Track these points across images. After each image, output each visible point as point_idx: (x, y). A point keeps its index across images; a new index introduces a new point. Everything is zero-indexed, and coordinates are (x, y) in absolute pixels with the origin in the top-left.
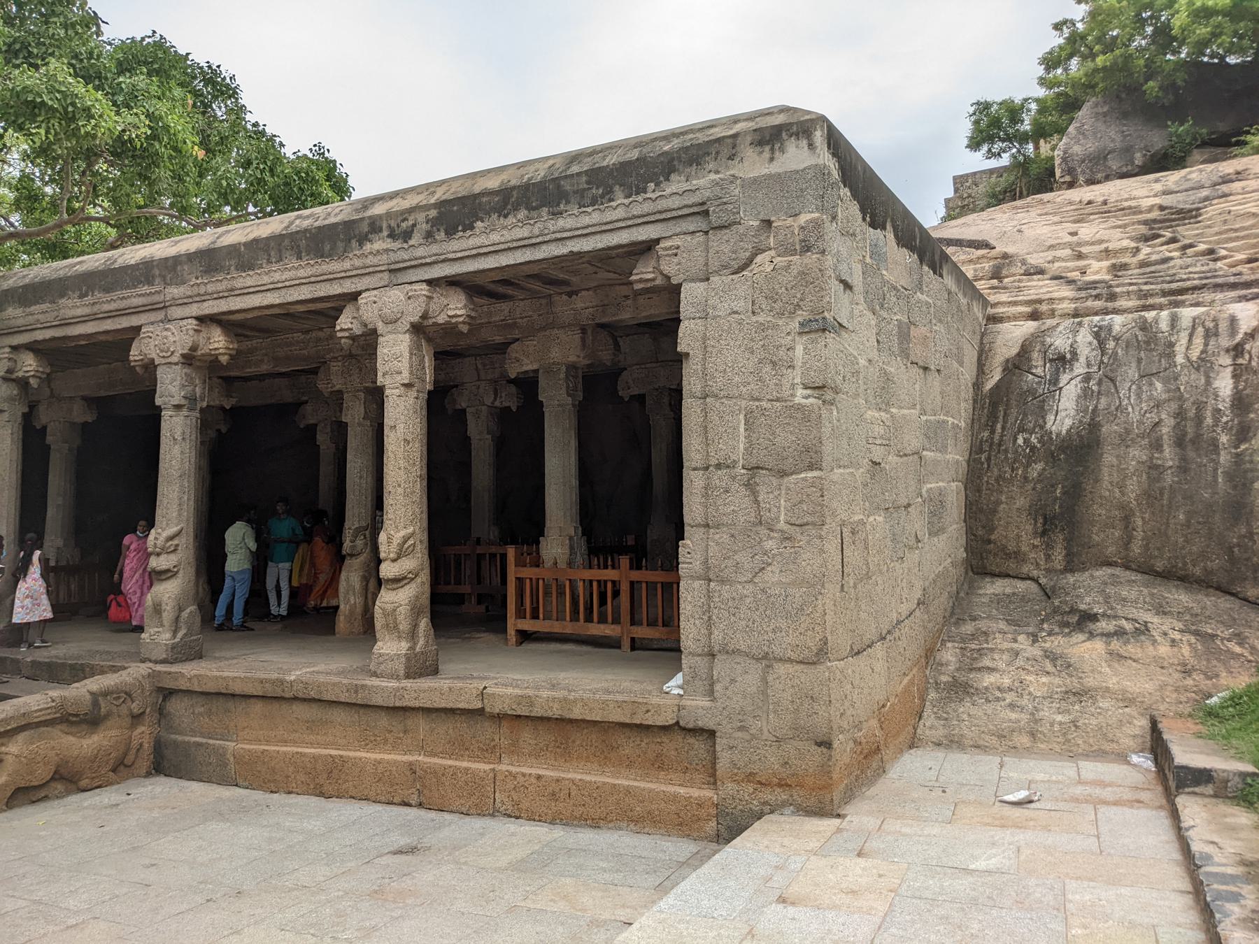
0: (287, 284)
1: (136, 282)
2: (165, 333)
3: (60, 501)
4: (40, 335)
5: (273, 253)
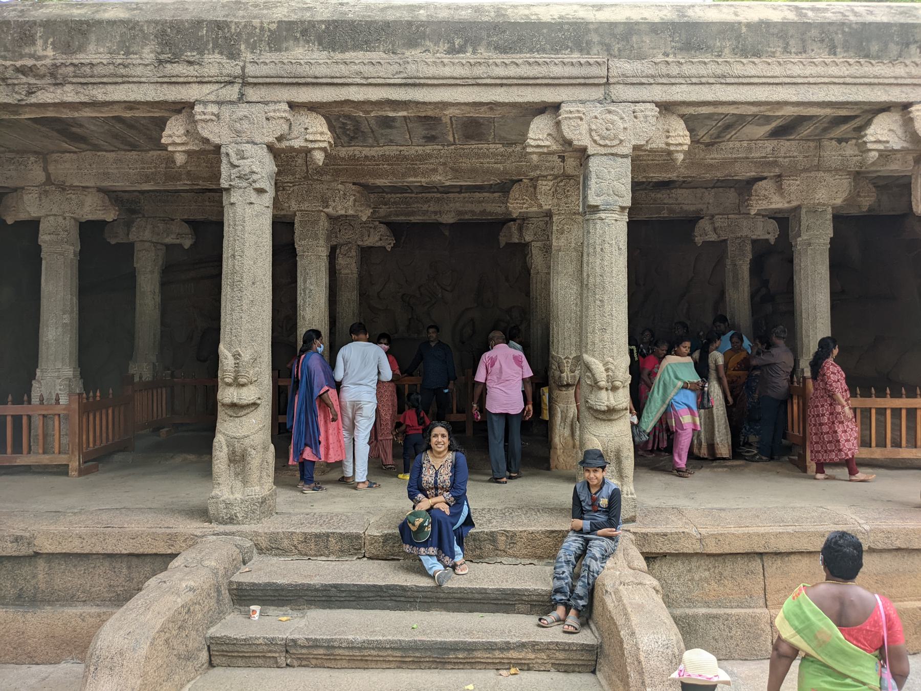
0: (812, 80)
1: (557, 46)
2: (609, 116)
3: (66, 319)
5: (792, 42)
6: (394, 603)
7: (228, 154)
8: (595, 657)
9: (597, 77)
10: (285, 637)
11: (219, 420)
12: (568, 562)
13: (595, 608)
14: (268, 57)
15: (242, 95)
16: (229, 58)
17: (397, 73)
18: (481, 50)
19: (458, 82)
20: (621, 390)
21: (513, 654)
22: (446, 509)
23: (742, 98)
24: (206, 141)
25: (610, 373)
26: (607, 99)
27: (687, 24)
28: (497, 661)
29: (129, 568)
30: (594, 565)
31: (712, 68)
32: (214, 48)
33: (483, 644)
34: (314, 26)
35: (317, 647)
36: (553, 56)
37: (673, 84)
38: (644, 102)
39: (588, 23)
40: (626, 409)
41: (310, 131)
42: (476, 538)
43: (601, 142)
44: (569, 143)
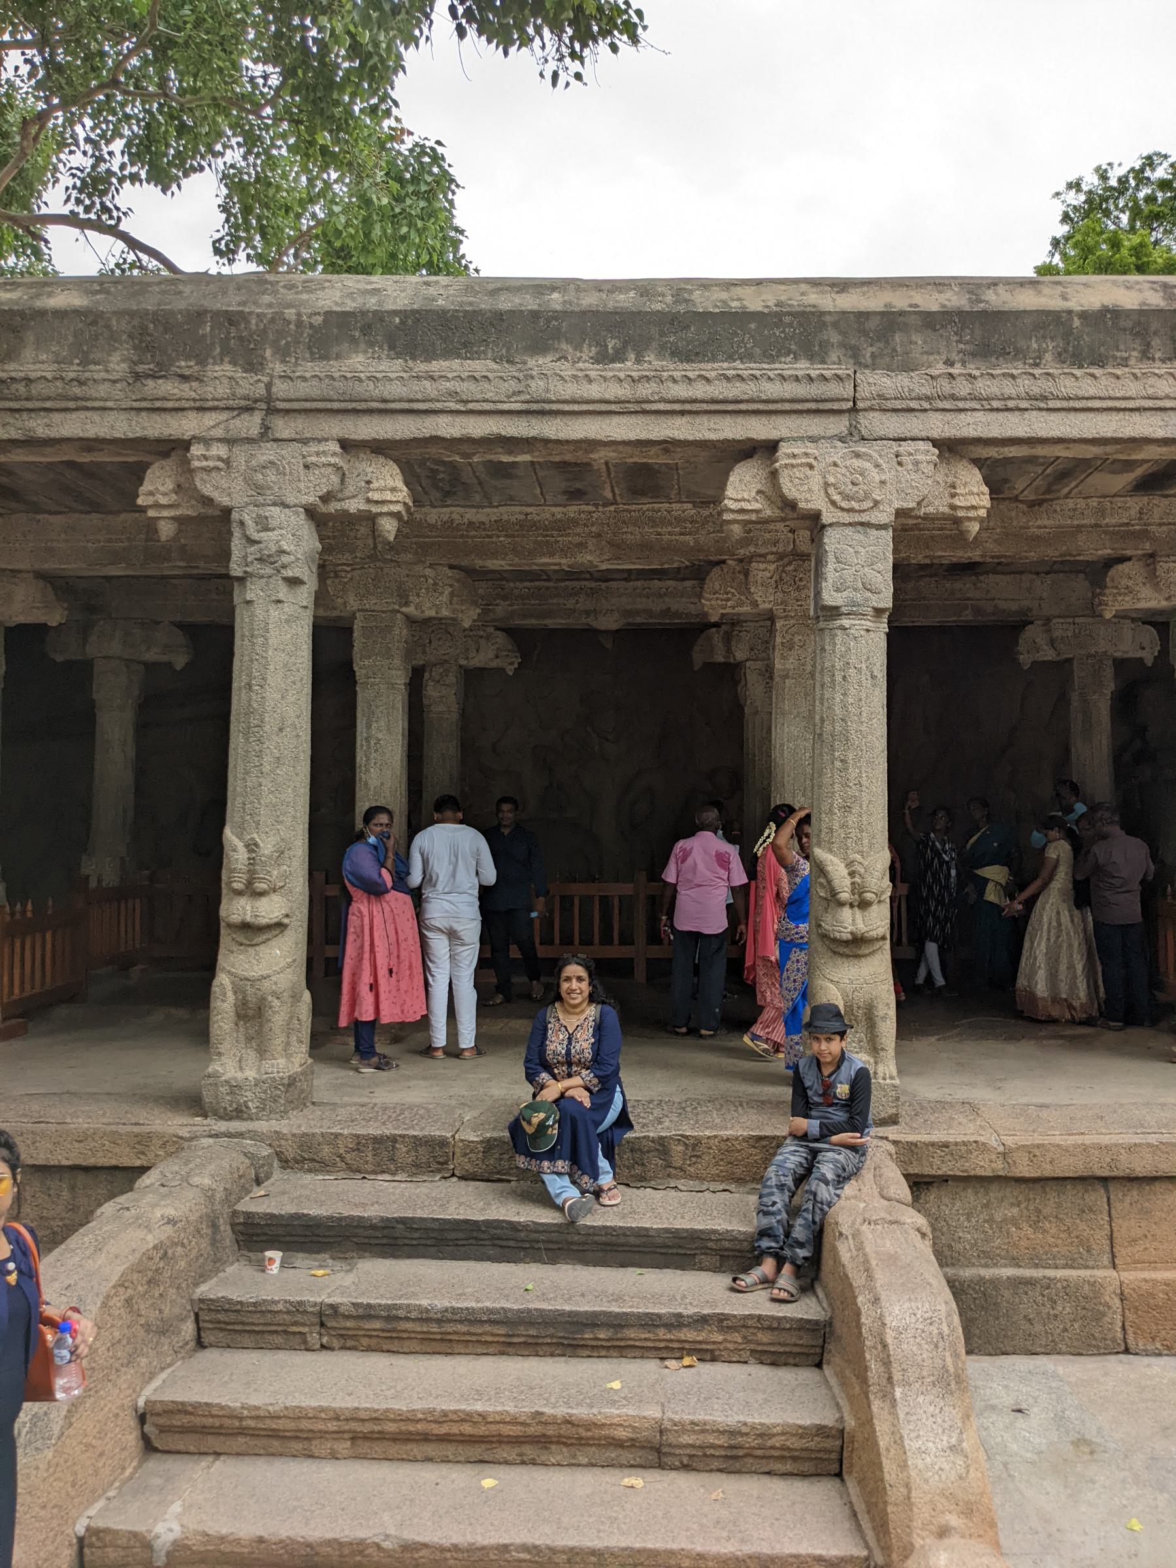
2: (856, 463)
4: (448, 427)
5: (1156, 342)
6: (498, 1250)
7: (242, 523)
8: (820, 1341)
9: (838, 400)
10: (319, 1300)
11: (222, 951)
12: (781, 1187)
13: (824, 1261)
14: (310, 368)
15: (266, 428)
16: (246, 371)
17: (514, 394)
18: (650, 357)
19: (613, 407)
20: (875, 907)
21: (688, 1335)
22: (585, 1098)
23: (1074, 433)
24: (208, 501)
25: (857, 879)
26: (854, 435)
27: (984, 313)
28: (662, 1345)
29: (72, 1188)
30: (824, 1192)
31: (1025, 385)
32: (222, 355)
33: (639, 1316)
34: (382, 320)
35: (370, 1317)
36: (766, 366)
37: (961, 410)
38: (913, 439)
39: (822, 313)
40: (883, 938)
41: (375, 485)
42: (635, 1147)
43: (844, 504)
44: (792, 505)
